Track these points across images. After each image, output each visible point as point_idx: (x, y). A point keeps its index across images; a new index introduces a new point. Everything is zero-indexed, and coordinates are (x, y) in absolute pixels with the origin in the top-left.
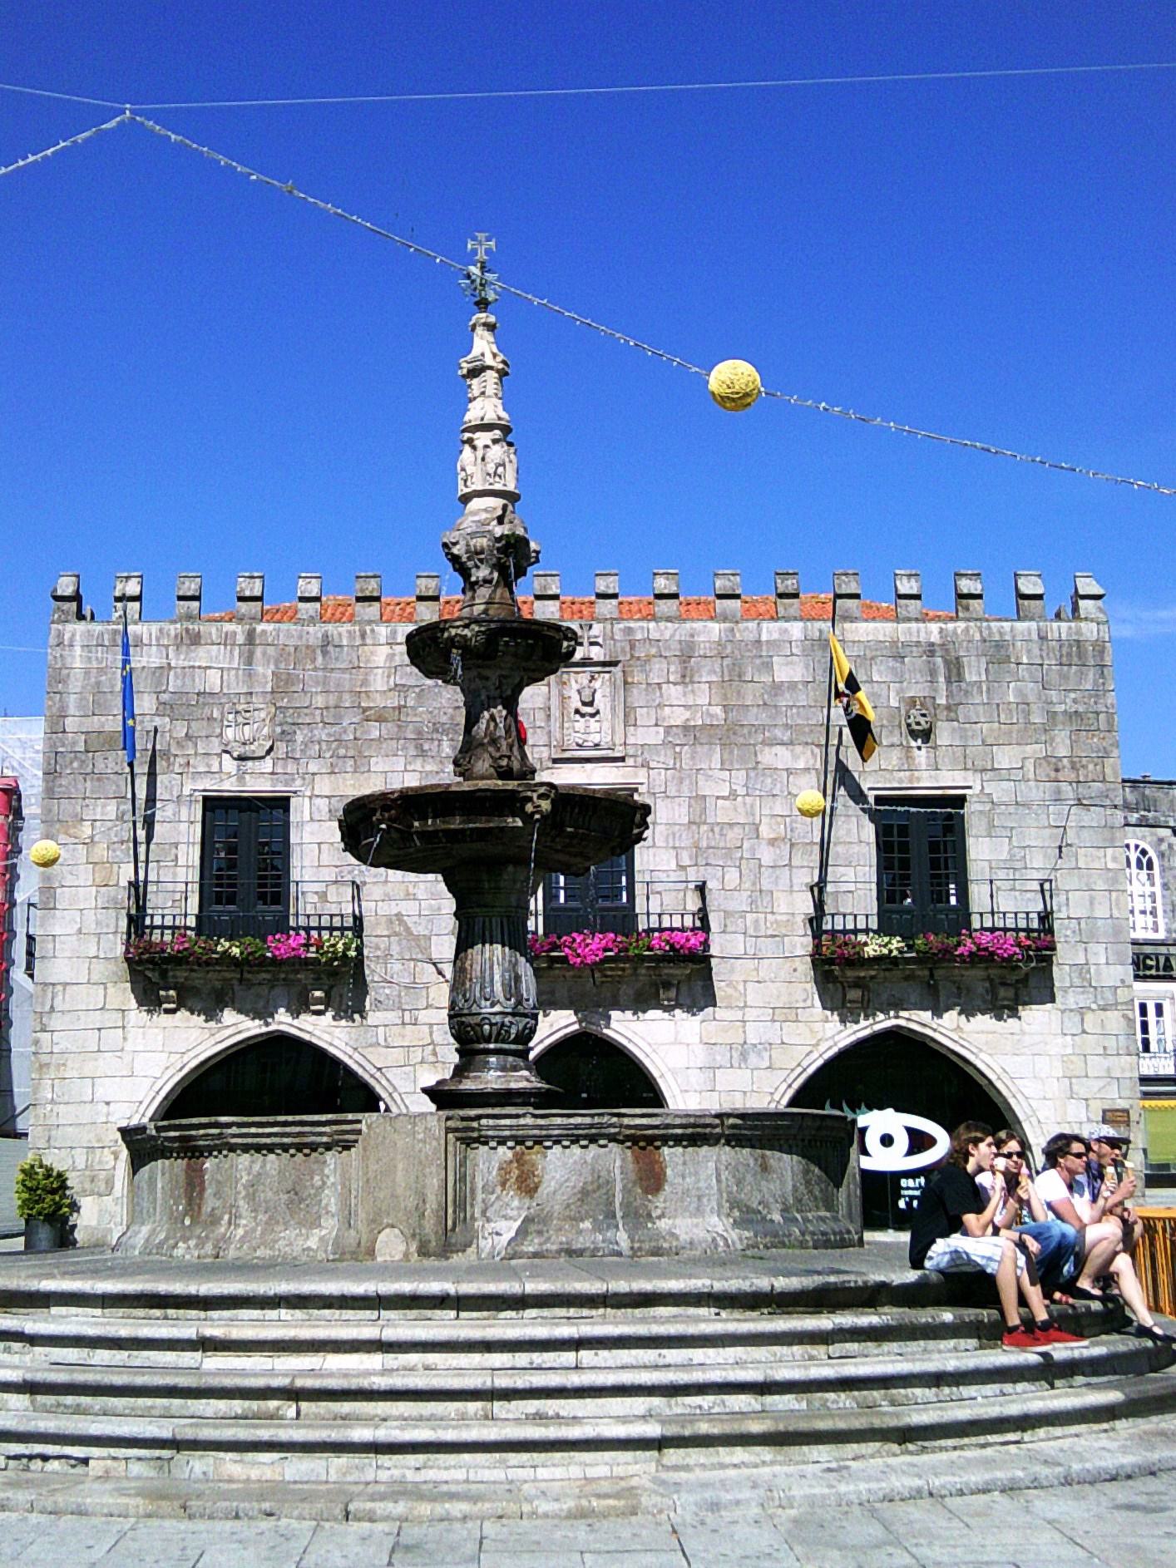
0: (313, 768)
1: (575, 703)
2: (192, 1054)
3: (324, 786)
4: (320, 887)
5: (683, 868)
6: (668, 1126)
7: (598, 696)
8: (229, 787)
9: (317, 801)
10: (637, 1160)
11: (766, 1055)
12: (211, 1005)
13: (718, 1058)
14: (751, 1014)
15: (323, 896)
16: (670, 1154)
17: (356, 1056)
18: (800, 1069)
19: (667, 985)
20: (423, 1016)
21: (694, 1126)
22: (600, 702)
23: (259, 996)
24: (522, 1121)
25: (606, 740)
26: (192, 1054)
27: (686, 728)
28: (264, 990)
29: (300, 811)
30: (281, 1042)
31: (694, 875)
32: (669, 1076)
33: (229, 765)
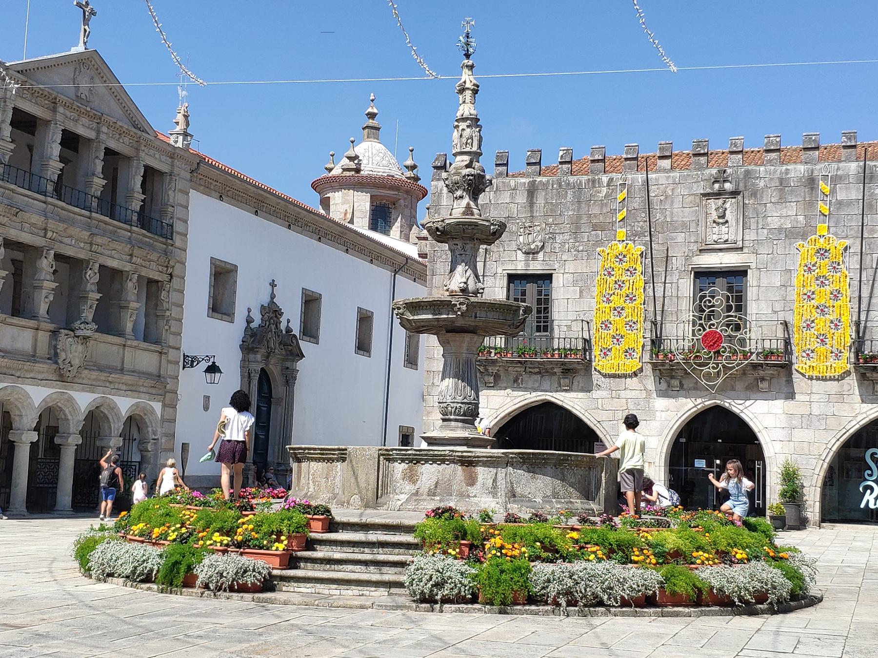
0: (564, 257)
1: (714, 215)
2: (501, 410)
3: (570, 267)
4: (569, 323)
5: (775, 312)
6: (478, 457)
7: (728, 212)
8: (520, 265)
9: (566, 276)
10: (464, 471)
11: (823, 422)
12: (516, 384)
13: (794, 422)
14: (815, 397)
15: (569, 327)
16: (480, 470)
17: (586, 414)
18: (844, 431)
19: (763, 379)
20: (623, 394)
21: (491, 457)
22: (729, 216)
23: (537, 381)
24: (409, 452)
25: (732, 237)
26: (501, 410)
27: (780, 230)
28: (538, 377)
29: (558, 281)
30: (548, 406)
31: (782, 316)
32: (764, 432)
33: (520, 256)
